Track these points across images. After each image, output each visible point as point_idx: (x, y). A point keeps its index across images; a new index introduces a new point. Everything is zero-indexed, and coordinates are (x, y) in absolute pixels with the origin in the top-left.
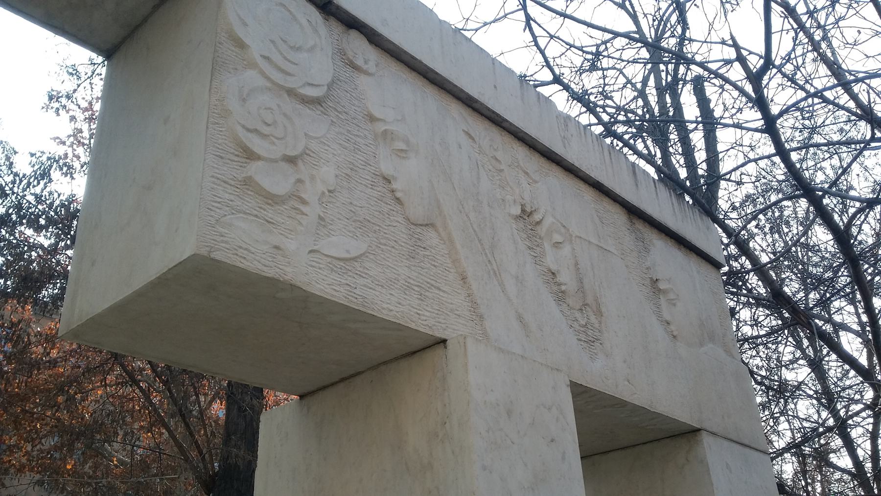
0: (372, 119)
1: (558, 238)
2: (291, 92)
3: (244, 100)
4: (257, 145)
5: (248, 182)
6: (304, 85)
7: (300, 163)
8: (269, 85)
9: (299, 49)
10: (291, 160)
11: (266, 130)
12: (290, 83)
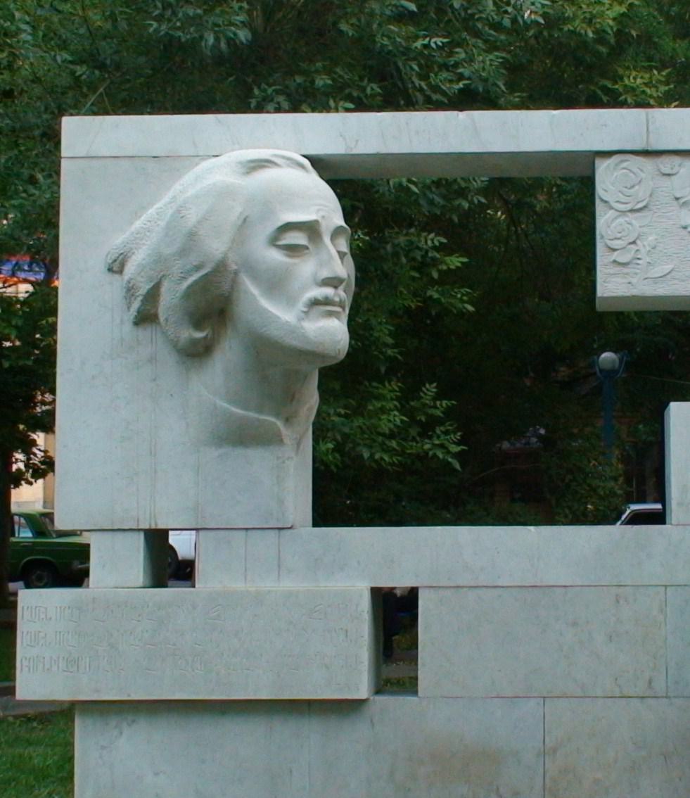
0: (677, 199)
2: (632, 211)
3: (609, 227)
5: (615, 261)
6: (636, 204)
7: (638, 242)
8: (618, 213)
9: (633, 187)
10: (634, 243)
11: (619, 235)
12: (629, 207)
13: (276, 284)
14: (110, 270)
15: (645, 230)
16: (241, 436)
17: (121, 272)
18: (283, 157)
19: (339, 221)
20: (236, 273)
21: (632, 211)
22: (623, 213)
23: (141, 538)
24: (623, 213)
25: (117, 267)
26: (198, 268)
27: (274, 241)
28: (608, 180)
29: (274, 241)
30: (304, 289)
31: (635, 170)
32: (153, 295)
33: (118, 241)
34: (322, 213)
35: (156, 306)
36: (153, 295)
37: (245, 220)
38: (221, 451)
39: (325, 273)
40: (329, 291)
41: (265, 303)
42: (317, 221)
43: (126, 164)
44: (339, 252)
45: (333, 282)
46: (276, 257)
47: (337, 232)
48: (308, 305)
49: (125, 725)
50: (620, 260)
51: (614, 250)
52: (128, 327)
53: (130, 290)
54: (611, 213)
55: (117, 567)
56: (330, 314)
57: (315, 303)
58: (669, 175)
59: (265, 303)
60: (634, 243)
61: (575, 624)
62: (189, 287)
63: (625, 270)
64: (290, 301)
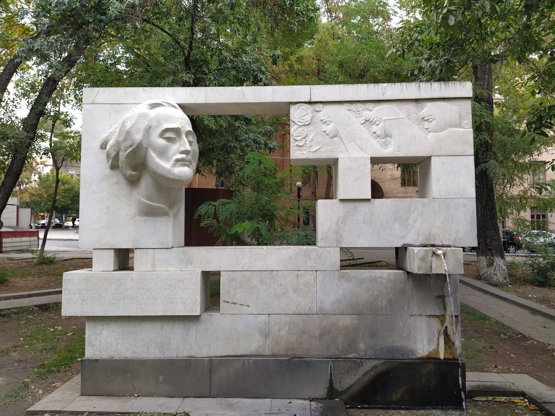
0: (322, 120)
1: (377, 123)
2: (304, 125)
4: (298, 138)
10: (304, 138)
13: (163, 153)
14: (101, 148)
15: (308, 133)
16: (149, 212)
17: (105, 148)
18: (166, 103)
19: (189, 128)
20: (147, 148)
21: (304, 125)
22: (301, 126)
23: (112, 252)
24: (301, 126)
25: (103, 146)
26: (131, 146)
27: (161, 135)
28: (295, 113)
29: (161, 135)
30: (174, 154)
31: (305, 109)
32: (117, 157)
33: (104, 136)
34: (181, 125)
35: (118, 162)
36: (117, 157)
37: (150, 127)
38: (144, 218)
39: (183, 149)
40: (184, 156)
41: (158, 160)
42: (179, 128)
43: (108, 105)
44: (189, 141)
45: (186, 152)
46: (162, 142)
47: (188, 134)
48: (177, 162)
49: (105, 325)
50: (300, 144)
51: (297, 141)
52: (108, 170)
53: (108, 156)
54: (296, 126)
55: (104, 263)
56: (184, 165)
57: (178, 160)
58: (319, 111)
59: (158, 160)
60: (304, 138)
61: (281, 285)
62: (128, 153)
63: (301, 148)
64: (168, 159)
